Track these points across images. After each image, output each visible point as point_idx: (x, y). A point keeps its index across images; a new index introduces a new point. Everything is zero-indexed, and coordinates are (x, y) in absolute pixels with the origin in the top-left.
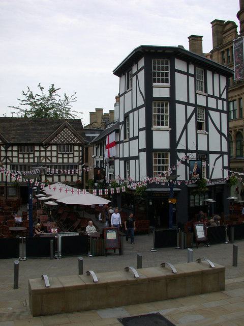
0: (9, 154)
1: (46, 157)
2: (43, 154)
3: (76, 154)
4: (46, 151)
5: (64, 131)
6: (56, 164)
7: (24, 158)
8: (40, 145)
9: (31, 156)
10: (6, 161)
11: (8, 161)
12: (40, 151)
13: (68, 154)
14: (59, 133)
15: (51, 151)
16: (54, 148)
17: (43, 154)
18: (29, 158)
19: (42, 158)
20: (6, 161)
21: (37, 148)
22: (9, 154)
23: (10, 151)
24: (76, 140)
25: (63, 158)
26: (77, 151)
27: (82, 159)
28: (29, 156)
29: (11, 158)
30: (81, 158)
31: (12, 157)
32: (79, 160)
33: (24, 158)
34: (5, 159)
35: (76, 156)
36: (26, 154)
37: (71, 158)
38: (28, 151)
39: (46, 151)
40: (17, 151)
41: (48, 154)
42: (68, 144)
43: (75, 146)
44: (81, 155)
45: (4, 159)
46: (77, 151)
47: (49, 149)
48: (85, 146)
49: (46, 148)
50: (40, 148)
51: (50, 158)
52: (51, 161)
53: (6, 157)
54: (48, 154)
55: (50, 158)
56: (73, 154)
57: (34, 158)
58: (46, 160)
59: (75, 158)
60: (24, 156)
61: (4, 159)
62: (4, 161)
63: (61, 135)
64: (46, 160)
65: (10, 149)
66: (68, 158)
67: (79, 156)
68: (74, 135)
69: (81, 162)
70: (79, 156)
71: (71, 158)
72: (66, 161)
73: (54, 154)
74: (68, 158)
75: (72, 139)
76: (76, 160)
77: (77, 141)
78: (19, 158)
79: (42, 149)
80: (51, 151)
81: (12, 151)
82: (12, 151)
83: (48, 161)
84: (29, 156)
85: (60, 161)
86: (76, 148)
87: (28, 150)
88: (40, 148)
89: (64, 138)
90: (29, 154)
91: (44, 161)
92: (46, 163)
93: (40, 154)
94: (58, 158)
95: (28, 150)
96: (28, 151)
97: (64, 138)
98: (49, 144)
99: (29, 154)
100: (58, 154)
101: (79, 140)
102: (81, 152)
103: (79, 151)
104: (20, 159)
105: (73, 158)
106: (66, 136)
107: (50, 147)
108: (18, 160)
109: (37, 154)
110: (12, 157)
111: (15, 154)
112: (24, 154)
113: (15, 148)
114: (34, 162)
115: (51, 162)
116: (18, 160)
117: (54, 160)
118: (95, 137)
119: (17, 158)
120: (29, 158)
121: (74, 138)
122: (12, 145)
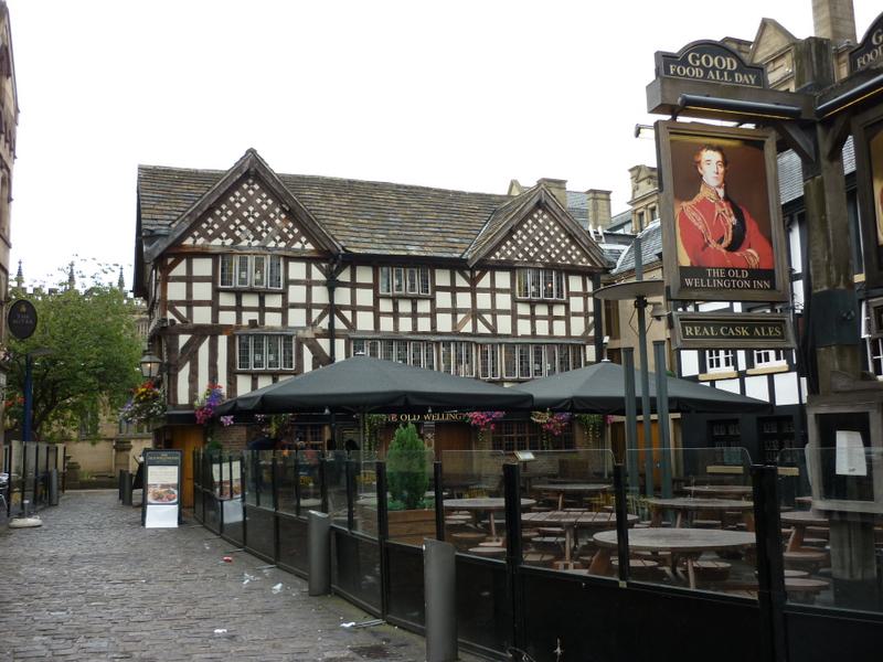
0: (343, 296)
1: (475, 314)
2: (464, 300)
3: (577, 304)
4: (473, 290)
5: (536, 222)
6: (511, 341)
7: (396, 315)
8: (456, 266)
9: (424, 307)
10: (331, 324)
11: (339, 324)
12: (453, 290)
13: (551, 305)
14: (519, 226)
15: (493, 291)
16: (503, 280)
17: (464, 300)
18: (414, 315)
19: (460, 317)
20: (331, 324)
21: (442, 278)
22: (343, 296)
23: (344, 285)
24: (576, 256)
25: (533, 318)
26: (577, 294)
27: (597, 324)
28: (414, 305)
29: (348, 314)
30: (591, 319)
31: (354, 308)
32: (588, 329)
33: (396, 315)
34: (326, 320)
35: (575, 314)
36: (405, 298)
37: (558, 318)
38: (413, 286)
39: (473, 290)
40: (374, 286)
41: (484, 301)
42: (551, 267)
43: (571, 278)
44: (591, 308)
45: (321, 317)
46: (577, 294)
47: (485, 282)
48: (603, 278)
49: (474, 281)
50: (453, 280)
51: (488, 318)
52: (493, 328)
53: (332, 309)
54: (484, 301)
55: (488, 318)
56: (567, 305)
57: (433, 315)
58: (475, 326)
59: (573, 319)
60: (396, 305)
61: (321, 317)
62: (324, 324)
63: (525, 232)
64: (475, 326)
65: (345, 276)
66: (551, 318)
67: (586, 314)
68: (569, 236)
69: (592, 333)
70: (586, 314)
71: (558, 318)
72: (542, 328)
73: (504, 301)
74: (551, 318)
75: (563, 251)
76: (578, 327)
77: (579, 258)
78: (377, 315)
79: (461, 282)
80: (493, 291)
81: (353, 285)
82: (353, 285)
83: (482, 329)
84: (414, 305)
85: (524, 328)
86: (575, 284)
87: (412, 281)
88: (453, 280)
89: (537, 244)
90: (414, 300)
91: (468, 328)
92: (475, 334)
93: (454, 300)
94: (515, 317)
95: (412, 281)
96: (413, 286)
97: (537, 244)
98: (486, 266)
99: (414, 300)
100: (515, 301)
101: (585, 254)
102: (590, 300)
103: (585, 295)
104: (382, 319)
105: (567, 318)
106: (541, 239)
107: (487, 276)
108: (377, 324)
109: (443, 300)
110: (354, 308)
111: (365, 298)
112: (395, 300)
113: (365, 275)
114: (434, 331)
115: (494, 334)
116: (377, 324)
117: (504, 325)
118: (619, 252)
119: (371, 314)
120: (414, 315)
121: (568, 247)
122: (354, 261)
